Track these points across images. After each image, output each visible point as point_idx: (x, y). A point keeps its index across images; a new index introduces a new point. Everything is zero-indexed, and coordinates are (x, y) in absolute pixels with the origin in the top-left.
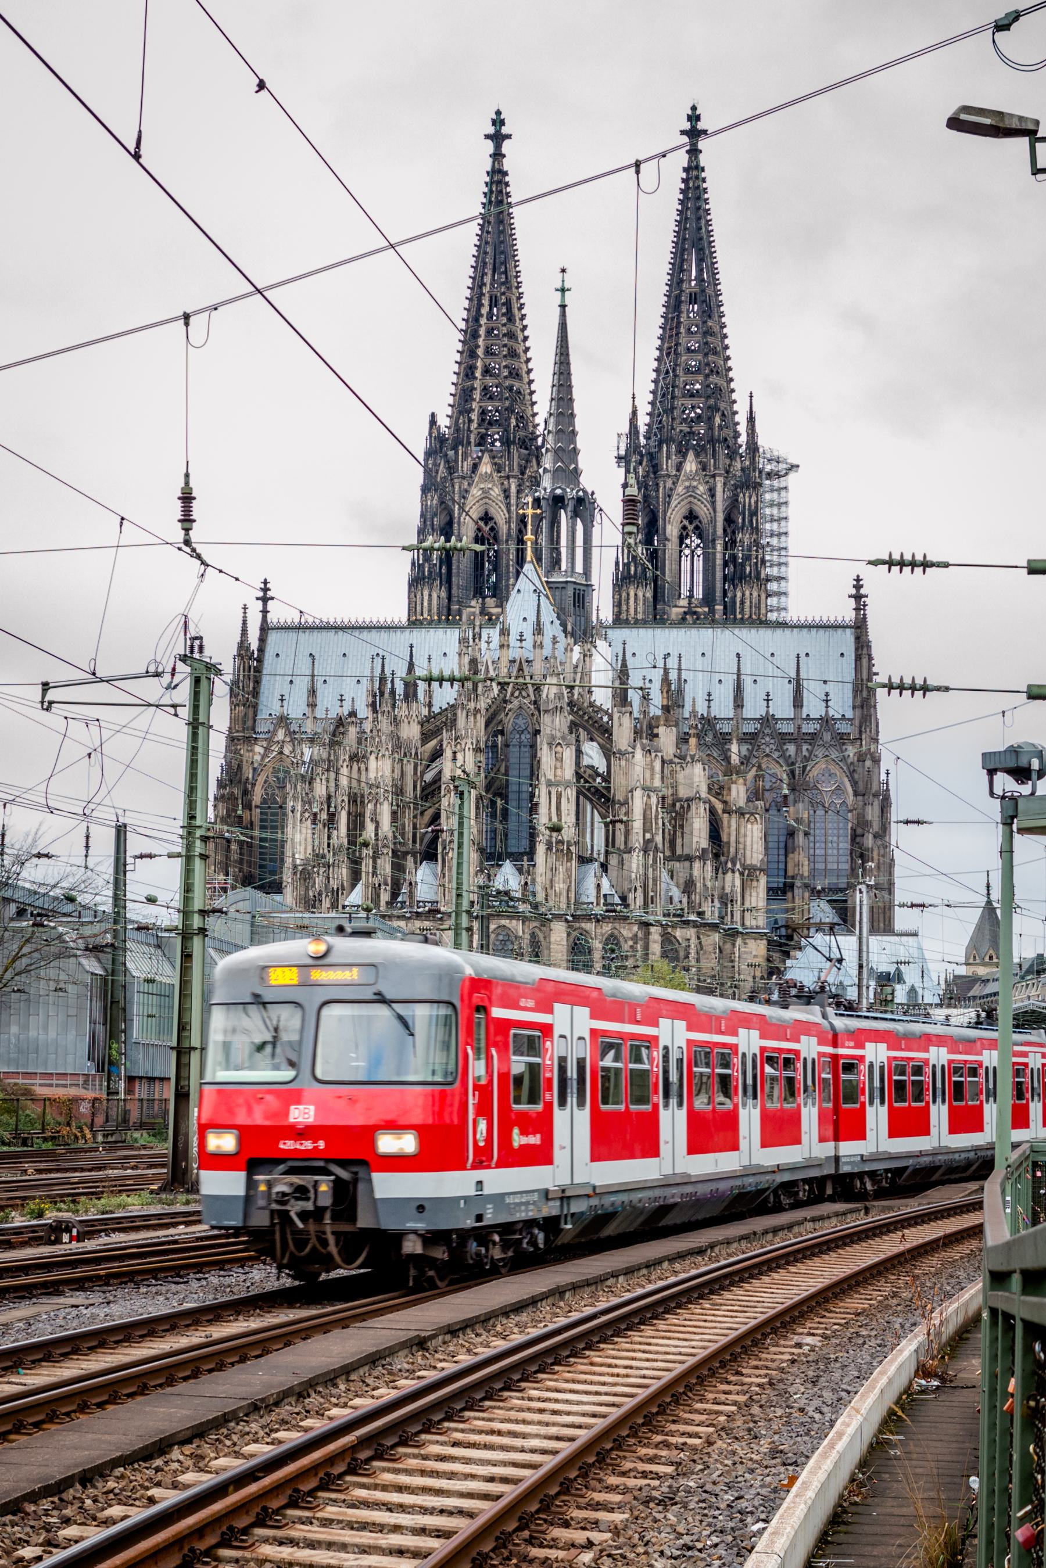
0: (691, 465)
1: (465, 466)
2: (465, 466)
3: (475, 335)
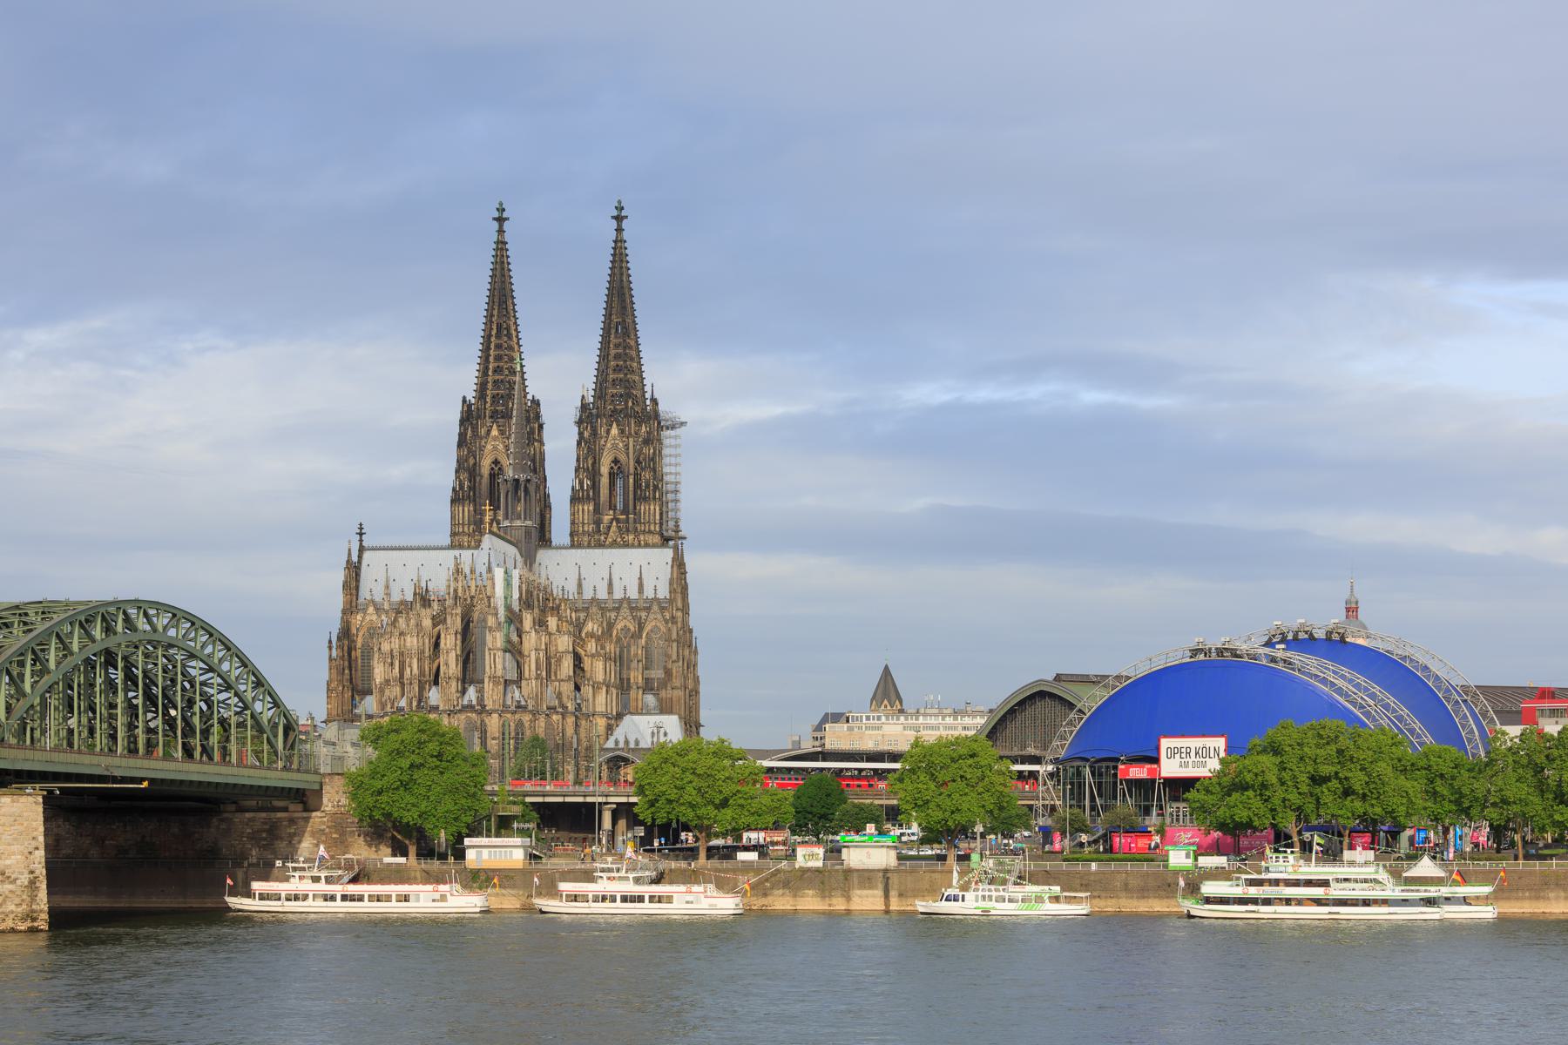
0: (614, 431)
1: (483, 432)
2: (483, 432)
3: (488, 348)
